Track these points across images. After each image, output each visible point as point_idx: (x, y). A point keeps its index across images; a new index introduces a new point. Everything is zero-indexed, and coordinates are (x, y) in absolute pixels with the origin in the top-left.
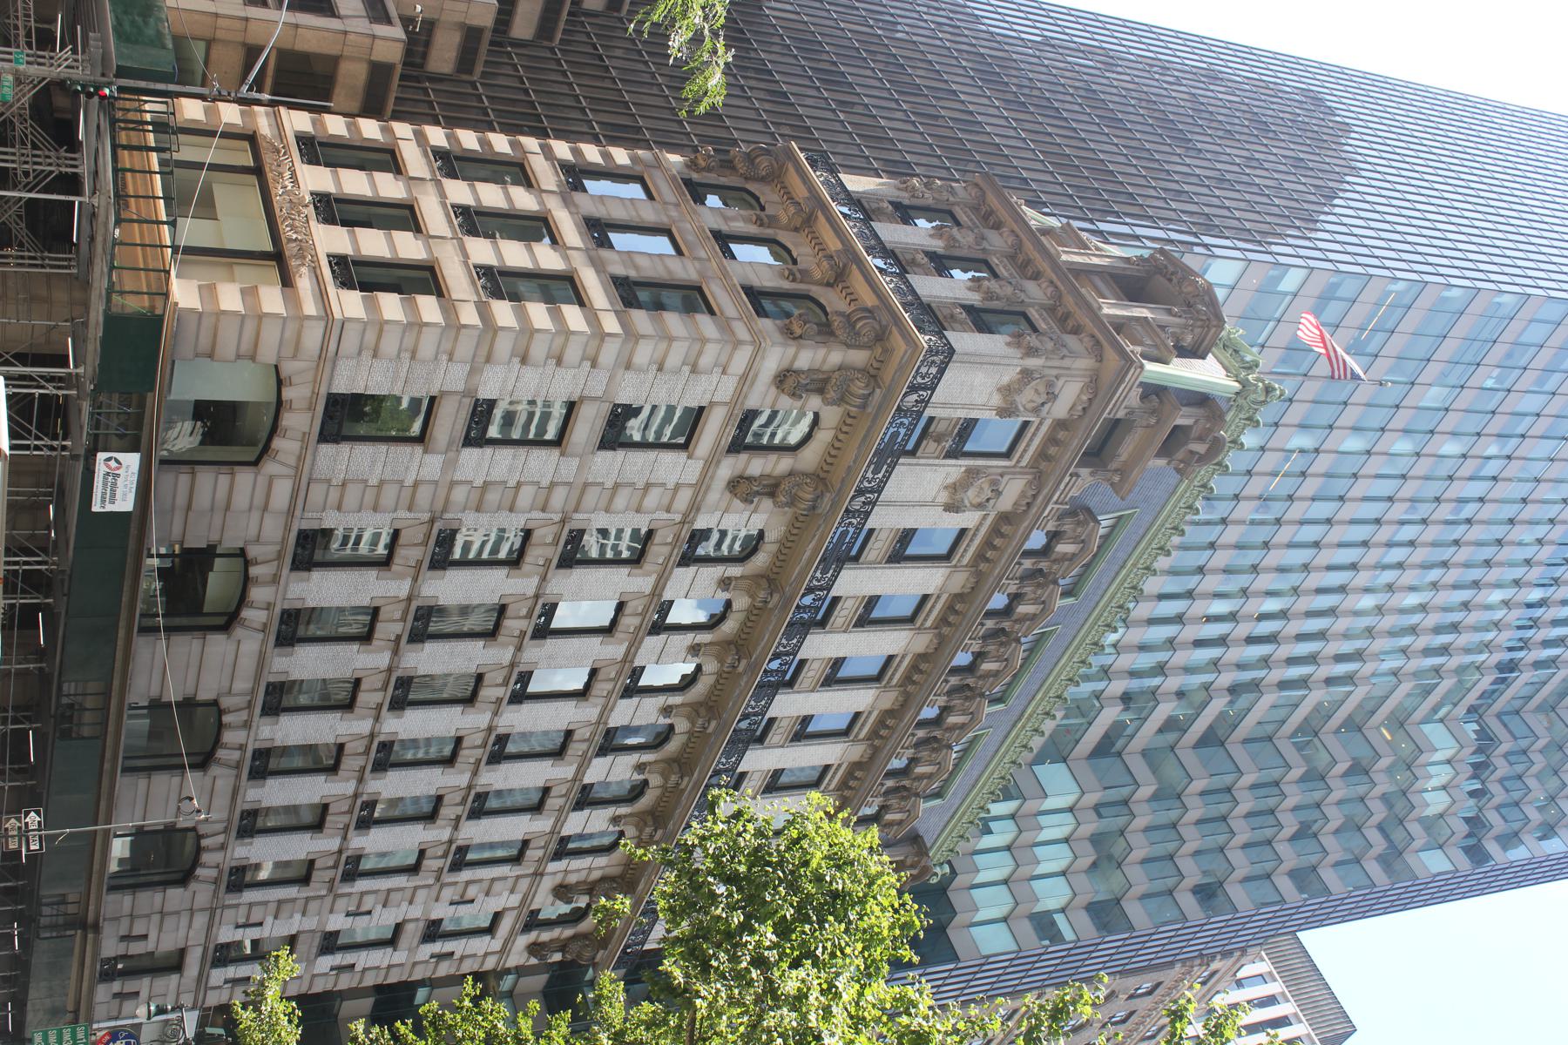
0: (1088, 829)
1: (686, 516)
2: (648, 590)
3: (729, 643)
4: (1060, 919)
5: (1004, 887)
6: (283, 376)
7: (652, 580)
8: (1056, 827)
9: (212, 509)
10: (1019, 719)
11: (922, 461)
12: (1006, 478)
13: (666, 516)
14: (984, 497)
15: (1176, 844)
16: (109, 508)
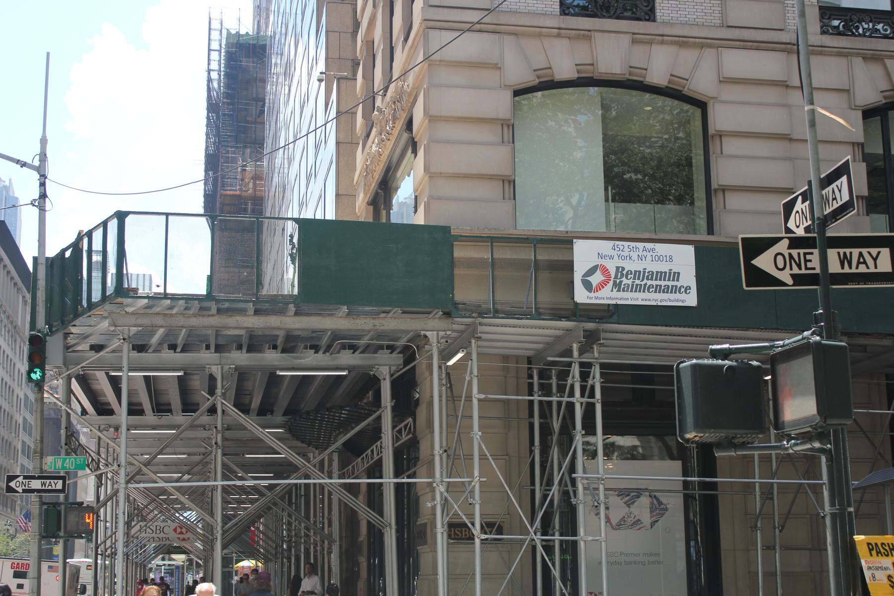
6: (530, 79)
9: (790, 159)
16: (689, 278)
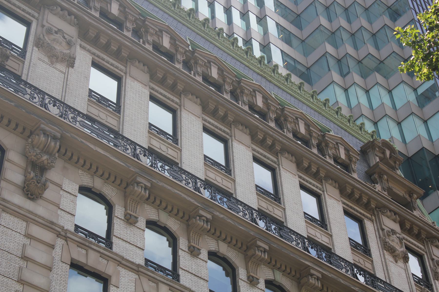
0: (357, 78)
1: (59, 235)
2: (133, 276)
3: (188, 226)
4: (420, 91)
5: (403, 124)
7: (123, 272)
8: (358, 97)
10: (265, 78)
11: (25, 71)
12: (45, 23)
13: (58, 250)
14: (61, 39)
15: (365, 33)
